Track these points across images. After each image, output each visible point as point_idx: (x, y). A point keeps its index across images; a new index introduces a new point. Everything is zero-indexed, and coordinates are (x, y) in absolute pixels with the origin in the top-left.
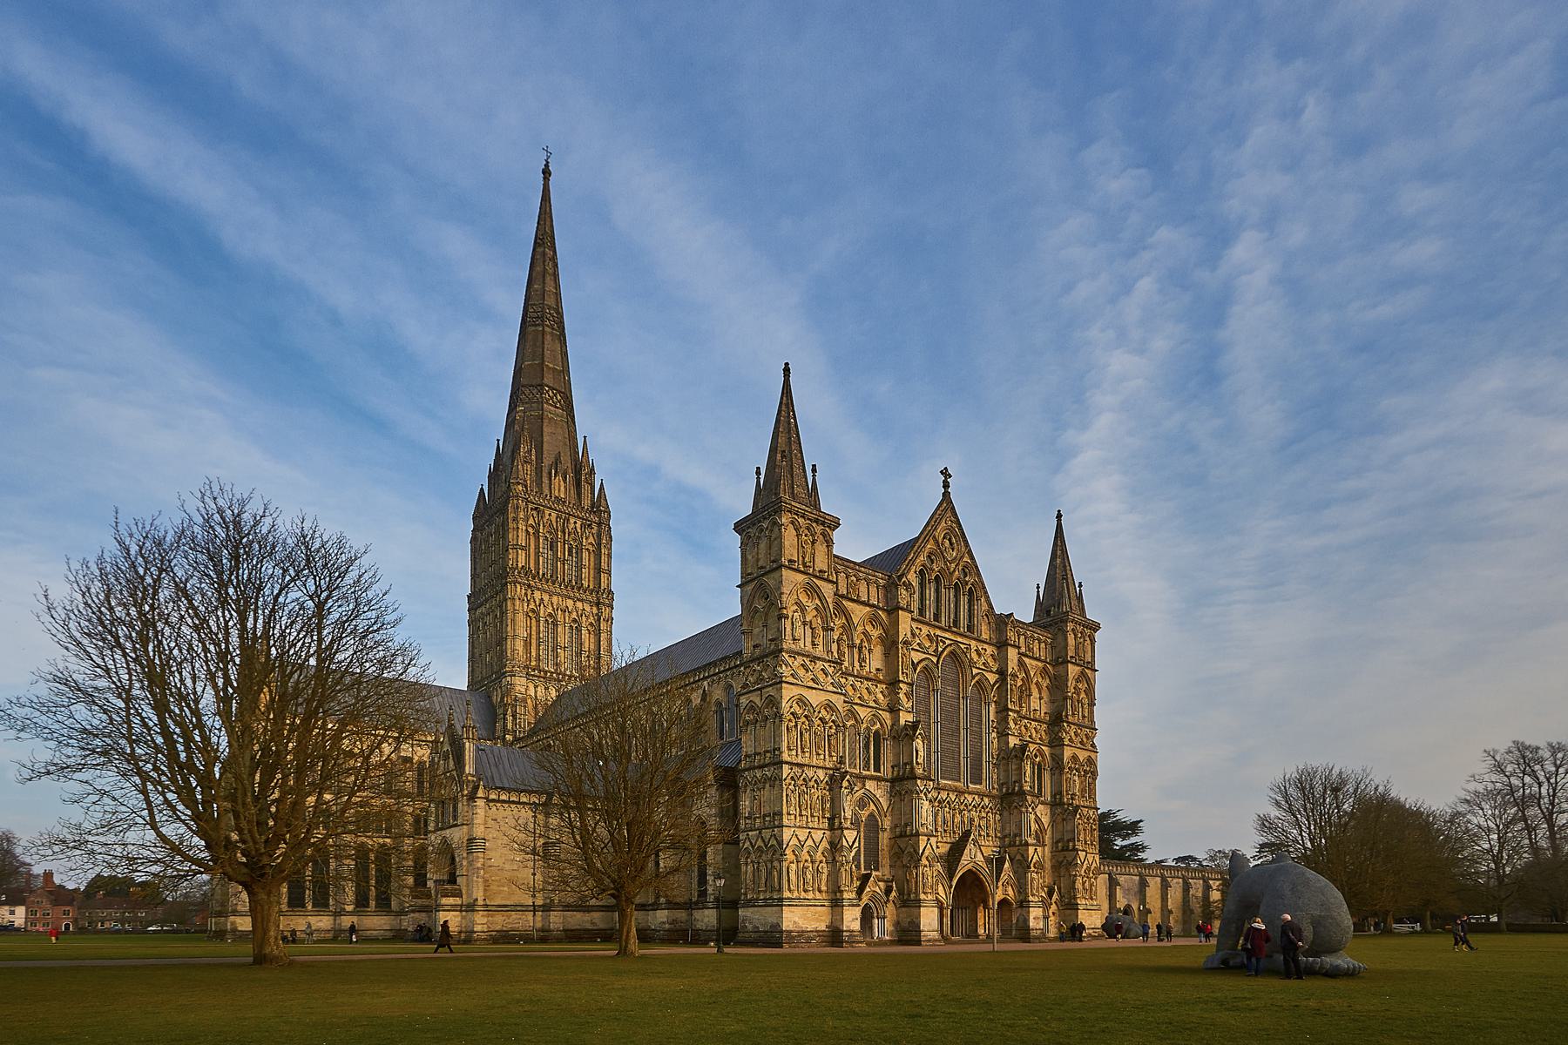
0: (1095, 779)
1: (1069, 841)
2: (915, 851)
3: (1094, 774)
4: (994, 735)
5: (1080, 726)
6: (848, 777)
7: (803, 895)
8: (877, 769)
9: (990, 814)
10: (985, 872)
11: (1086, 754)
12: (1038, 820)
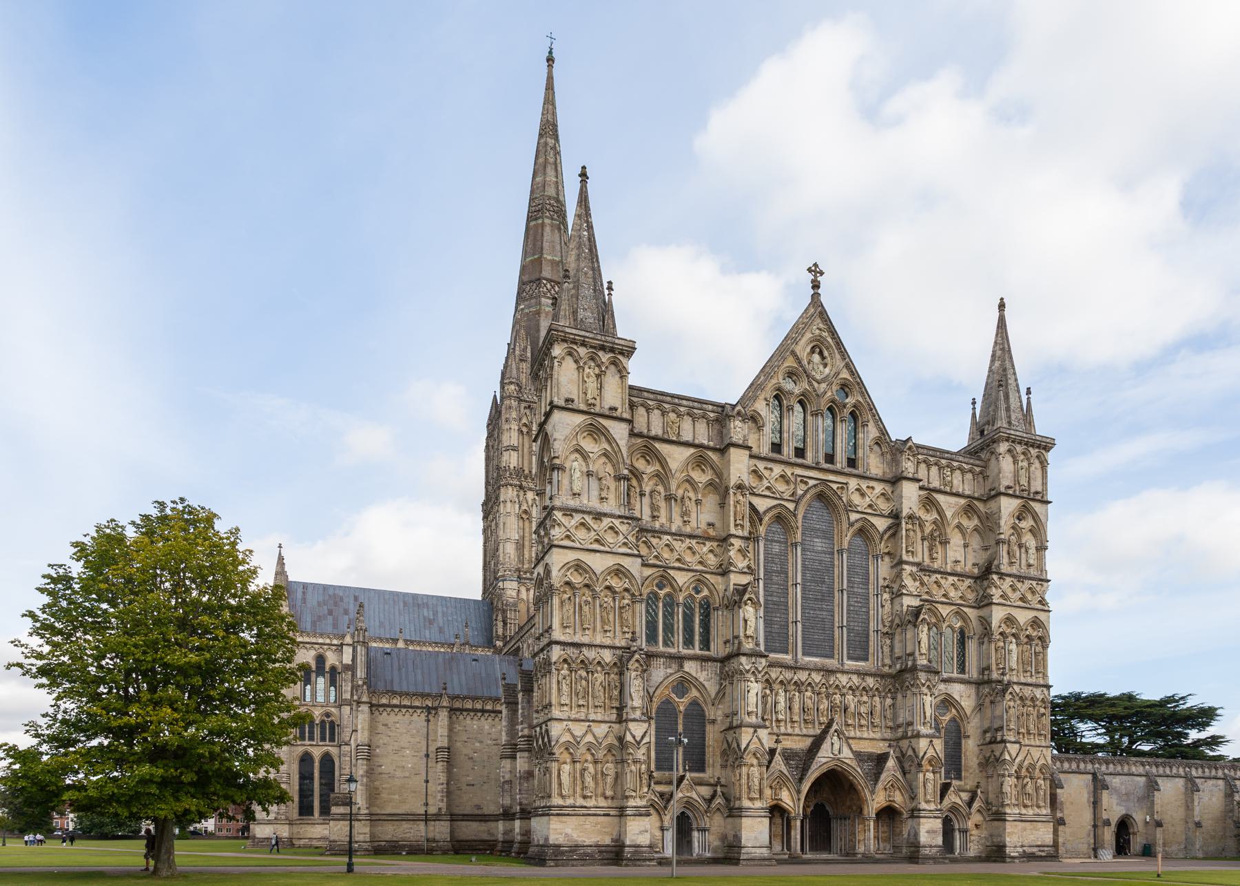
0: (1045, 647)
1: (997, 730)
2: (738, 746)
3: (1044, 641)
4: (886, 596)
5: (1021, 578)
6: (637, 656)
7: (580, 802)
8: (706, 644)
9: (877, 699)
10: (858, 772)
11: (1031, 614)
12: (947, 702)
